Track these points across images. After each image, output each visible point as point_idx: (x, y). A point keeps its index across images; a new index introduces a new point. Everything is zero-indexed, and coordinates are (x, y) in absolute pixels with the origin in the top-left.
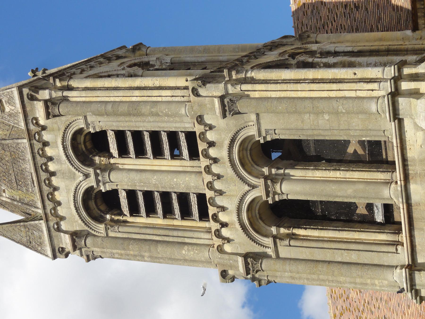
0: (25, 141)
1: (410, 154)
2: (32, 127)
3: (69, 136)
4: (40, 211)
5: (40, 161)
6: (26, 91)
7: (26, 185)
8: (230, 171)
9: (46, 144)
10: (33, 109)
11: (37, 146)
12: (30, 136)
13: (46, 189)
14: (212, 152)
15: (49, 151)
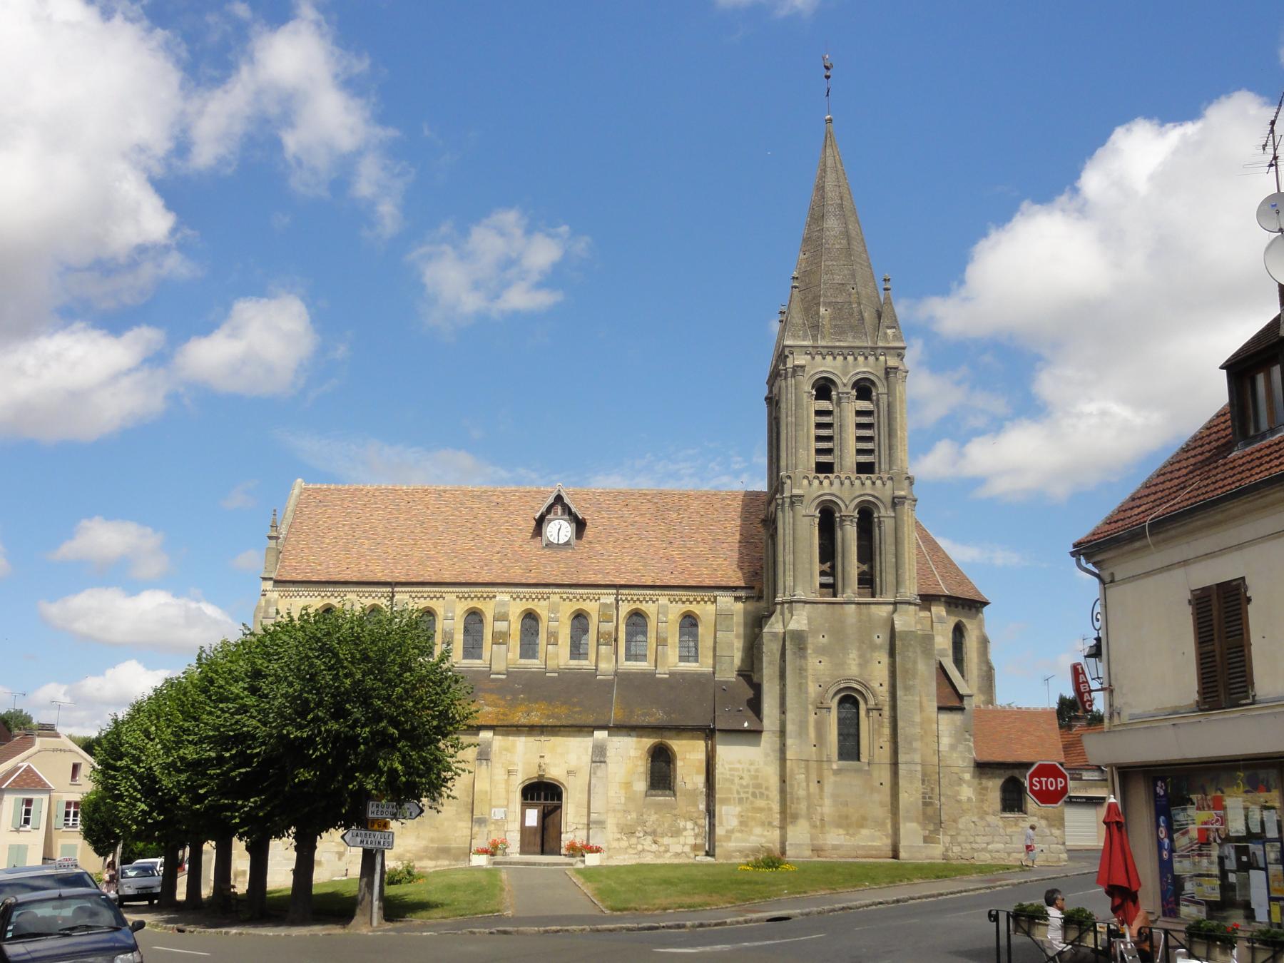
0: (870, 344)
1: (873, 607)
2: (879, 351)
3: (872, 378)
4: (820, 343)
5: (856, 351)
7: (835, 333)
8: (858, 493)
9: (866, 358)
10: (892, 355)
11: (867, 352)
12: (872, 349)
13: (836, 351)
14: (868, 483)
15: (861, 359)
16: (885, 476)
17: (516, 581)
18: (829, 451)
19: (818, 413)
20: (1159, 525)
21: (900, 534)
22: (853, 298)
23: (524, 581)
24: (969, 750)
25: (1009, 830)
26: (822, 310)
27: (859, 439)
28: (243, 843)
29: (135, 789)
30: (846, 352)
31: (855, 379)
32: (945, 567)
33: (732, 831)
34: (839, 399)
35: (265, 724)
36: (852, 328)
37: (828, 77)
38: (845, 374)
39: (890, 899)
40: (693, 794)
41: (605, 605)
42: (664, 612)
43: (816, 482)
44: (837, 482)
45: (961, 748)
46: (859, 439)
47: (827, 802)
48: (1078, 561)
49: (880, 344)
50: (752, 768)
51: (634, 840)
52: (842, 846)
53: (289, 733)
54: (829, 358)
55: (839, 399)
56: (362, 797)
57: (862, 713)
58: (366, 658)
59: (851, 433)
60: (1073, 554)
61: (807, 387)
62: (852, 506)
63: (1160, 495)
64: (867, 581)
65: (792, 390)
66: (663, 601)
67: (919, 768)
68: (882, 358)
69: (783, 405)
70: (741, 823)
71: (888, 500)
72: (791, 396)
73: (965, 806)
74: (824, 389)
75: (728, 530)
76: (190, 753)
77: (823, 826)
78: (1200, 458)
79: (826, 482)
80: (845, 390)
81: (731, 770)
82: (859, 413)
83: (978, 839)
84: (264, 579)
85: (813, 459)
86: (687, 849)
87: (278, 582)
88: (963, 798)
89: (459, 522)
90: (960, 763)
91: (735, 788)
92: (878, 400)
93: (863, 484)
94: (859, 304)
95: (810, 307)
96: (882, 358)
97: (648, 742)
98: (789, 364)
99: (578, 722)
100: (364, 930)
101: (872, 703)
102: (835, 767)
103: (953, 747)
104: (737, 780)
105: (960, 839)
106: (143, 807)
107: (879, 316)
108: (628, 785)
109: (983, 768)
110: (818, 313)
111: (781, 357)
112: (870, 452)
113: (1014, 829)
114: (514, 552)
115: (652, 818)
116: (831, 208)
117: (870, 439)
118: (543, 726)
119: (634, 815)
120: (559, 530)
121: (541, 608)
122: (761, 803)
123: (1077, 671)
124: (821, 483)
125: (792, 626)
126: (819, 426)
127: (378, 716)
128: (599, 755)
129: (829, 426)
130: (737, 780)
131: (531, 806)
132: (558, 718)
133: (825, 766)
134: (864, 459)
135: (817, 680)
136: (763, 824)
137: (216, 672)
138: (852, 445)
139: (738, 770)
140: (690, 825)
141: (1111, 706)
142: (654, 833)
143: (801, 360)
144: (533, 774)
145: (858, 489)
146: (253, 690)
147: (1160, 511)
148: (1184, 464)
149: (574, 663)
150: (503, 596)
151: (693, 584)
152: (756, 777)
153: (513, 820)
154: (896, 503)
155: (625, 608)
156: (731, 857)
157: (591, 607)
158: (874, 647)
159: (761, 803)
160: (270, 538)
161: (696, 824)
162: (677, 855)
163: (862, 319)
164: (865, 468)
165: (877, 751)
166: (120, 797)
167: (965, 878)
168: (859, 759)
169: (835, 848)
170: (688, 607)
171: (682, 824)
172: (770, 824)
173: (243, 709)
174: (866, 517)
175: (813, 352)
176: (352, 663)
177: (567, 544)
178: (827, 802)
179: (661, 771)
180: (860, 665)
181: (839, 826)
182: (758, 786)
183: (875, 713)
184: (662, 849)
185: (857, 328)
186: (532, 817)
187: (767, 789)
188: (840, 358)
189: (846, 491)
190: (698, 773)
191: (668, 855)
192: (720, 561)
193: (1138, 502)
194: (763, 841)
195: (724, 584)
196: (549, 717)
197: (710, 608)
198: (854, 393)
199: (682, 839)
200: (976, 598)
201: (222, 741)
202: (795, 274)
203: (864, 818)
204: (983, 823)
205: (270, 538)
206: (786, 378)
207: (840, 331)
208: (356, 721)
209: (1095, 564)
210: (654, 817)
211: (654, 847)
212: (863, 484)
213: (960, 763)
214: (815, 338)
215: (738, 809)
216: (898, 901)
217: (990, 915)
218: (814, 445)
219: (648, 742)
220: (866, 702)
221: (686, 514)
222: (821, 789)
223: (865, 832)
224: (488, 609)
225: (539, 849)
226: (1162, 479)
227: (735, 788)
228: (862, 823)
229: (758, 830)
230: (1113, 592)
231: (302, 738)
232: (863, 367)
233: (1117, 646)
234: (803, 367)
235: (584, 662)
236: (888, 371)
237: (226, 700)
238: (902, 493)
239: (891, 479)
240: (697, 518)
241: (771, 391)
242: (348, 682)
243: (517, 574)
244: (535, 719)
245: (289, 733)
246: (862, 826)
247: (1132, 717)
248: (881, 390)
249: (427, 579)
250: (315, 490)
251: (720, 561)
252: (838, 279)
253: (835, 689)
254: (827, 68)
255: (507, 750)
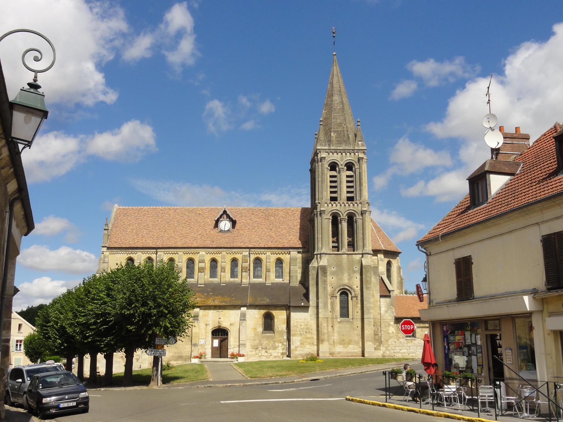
0: (352, 148)
4: (332, 148)
5: (346, 151)
6: (365, 151)
7: (338, 144)
12: (353, 150)
13: (338, 151)
14: (351, 205)
15: (348, 154)
16: (358, 202)
17: (208, 246)
18: (335, 192)
19: (331, 177)
20: (444, 236)
21: (364, 226)
22: (345, 129)
23: (211, 246)
24: (393, 313)
25: (409, 344)
26: (332, 134)
27: (348, 187)
28: (103, 355)
29: (56, 334)
30: (342, 151)
31: (346, 162)
32: (383, 238)
33: (297, 347)
34: (339, 171)
35: (114, 309)
36: (345, 141)
37: (334, 37)
38: (342, 160)
39: (358, 372)
40: (281, 332)
41: (245, 256)
42: (269, 258)
43: (330, 205)
44: (339, 205)
45: (389, 312)
46: (348, 187)
47: (336, 334)
48: (418, 247)
49: (356, 148)
50: (305, 321)
51: (258, 351)
52: (342, 352)
53: (125, 312)
54: (335, 154)
55: (339, 171)
56: (154, 336)
57: (350, 298)
58: (154, 283)
59: (344, 184)
60: (416, 245)
61: (326, 166)
62: (345, 214)
63: (447, 224)
64: (352, 245)
65: (320, 167)
66: (269, 253)
67: (372, 320)
68: (357, 154)
69: (317, 174)
70: (301, 344)
71: (360, 212)
72: (320, 170)
73: (391, 335)
74: (333, 166)
75: (295, 224)
76: (82, 320)
77: (334, 344)
78: (461, 210)
79: (334, 205)
80: (342, 167)
81: (297, 322)
82: (347, 176)
83: (396, 348)
84: (103, 247)
85: (329, 195)
86: (279, 354)
87: (109, 248)
88: (390, 332)
89: (184, 221)
90: (389, 318)
91: (298, 330)
92: (355, 171)
93: (349, 205)
94: (347, 131)
95: (328, 132)
96: (357, 154)
97: (263, 312)
98: (319, 157)
99: (234, 304)
100: (155, 387)
101: (353, 294)
102: (339, 320)
103: (386, 311)
104: (299, 326)
105: (389, 348)
106: (60, 341)
107: (356, 135)
108: (255, 329)
109: (398, 320)
110: (330, 135)
111: (316, 154)
112: (352, 192)
113: (411, 344)
114: (207, 234)
115: (265, 342)
116: (336, 91)
117: (352, 187)
118: (220, 306)
119: (258, 341)
120: (225, 225)
121: (218, 257)
122: (309, 335)
123: (418, 287)
124: (332, 205)
125: (321, 264)
126: (331, 182)
127: (159, 306)
128: (243, 317)
129: (335, 182)
130: (299, 326)
131: (215, 338)
132: (226, 302)
133: (335, 320)
134: (349, 195)
135: (332, 285)
136: (310, 344)
137: (91, 288)
138: (345, 189)
139: (299, 322)
140: (280, 345)
141: (430, 299)
142: (266, 348)
143: (324, 155)
144: (216, 325)
145: (347, 208)
146: (108, 295)
147: (445, 231)
148: (456, 212)
149: (232, 280)
150: (202, 252)
151: (280, 246)
152: (307, 325)
153: (208, 344)
154: (363, 213)
155: (253, 257)
156: (297, 357)
157: (239, 257)
158: (354, 272)
159: (309, 335)
160: (105, 230)
161: (283, 344)
162: (275, 357)
163: (349, 138)
164: (350, 199)
165: (355, 313)
166: (49, 338)
167: (390, 363)
168: (348, 317)
169: (339, 353)
170: (279, 256)
171: (277, 344)
172: (313, 344)
173: (105, 303)
174: (351, 218)
175: (329, 151)
176: (149, 284)
177: (229, 230)
178: (336, 334)
179: (268, 323)
180: (348, 279)
181: (341, 344)
182: (308, 329)
183: (355, 299)
184: (269, 355)
185: (347, 142)
186: (216, 343)
187: (311, 330)
188: (340, 154)
189: (343, 208)
190: (283, 324)
191: (272, 357)
192: (292, 237)
193: (439, 226)
194: (310, 351)
195: (293, 246)
196: (222, 302)
197: (288, 256)
198: (345, 168)
199: (277, 351)
200: (396, 251)
201: (97, 316)
202: (321, 119)
203: (351, 341)
204: (399, 342)
205: (105, 230)
206: (318, 162)
207: (339, 143)
208: (151, 307)
209: (424, 249)
210: (266, 342)
211: (266, 354)
212: (349, 205)
213: (389, 318)
214: (329, 146)
215: (300, 338)
216: (361, 373)
217: (383, 373)
218: (329, 190)
219: (263, 312)
220: (351, 294)
221: (278, 217)
222: (333, 329)
223: (351, 346)
224: (196, 258)
225: (219, 356)
226: (448, 217)
227: (298, 330)
228: (349, 343)
229: (308, 346)
230: (431, 258)
231: (130, 313)
232: (349, 158)
233: (432, 278)
234: (325, 158)
235: (236, 279)
236: (359, 159)
237: (97, 300)
238: (365, 209)
239: (360, 203)
240: (281, 218)
241: (312, 167)
242: (148, 292)
243: (208, 243)
244: (217, 303)
245: (125, 312)
246: (349, 344)
247: (437, 303)
248: (357, 167)
249: (171, 246)
250: (123, 209)
251: (292, 237)
252: (339, 121)
253: (339, 289)
254: (334, 33)
255: (205, 316)
